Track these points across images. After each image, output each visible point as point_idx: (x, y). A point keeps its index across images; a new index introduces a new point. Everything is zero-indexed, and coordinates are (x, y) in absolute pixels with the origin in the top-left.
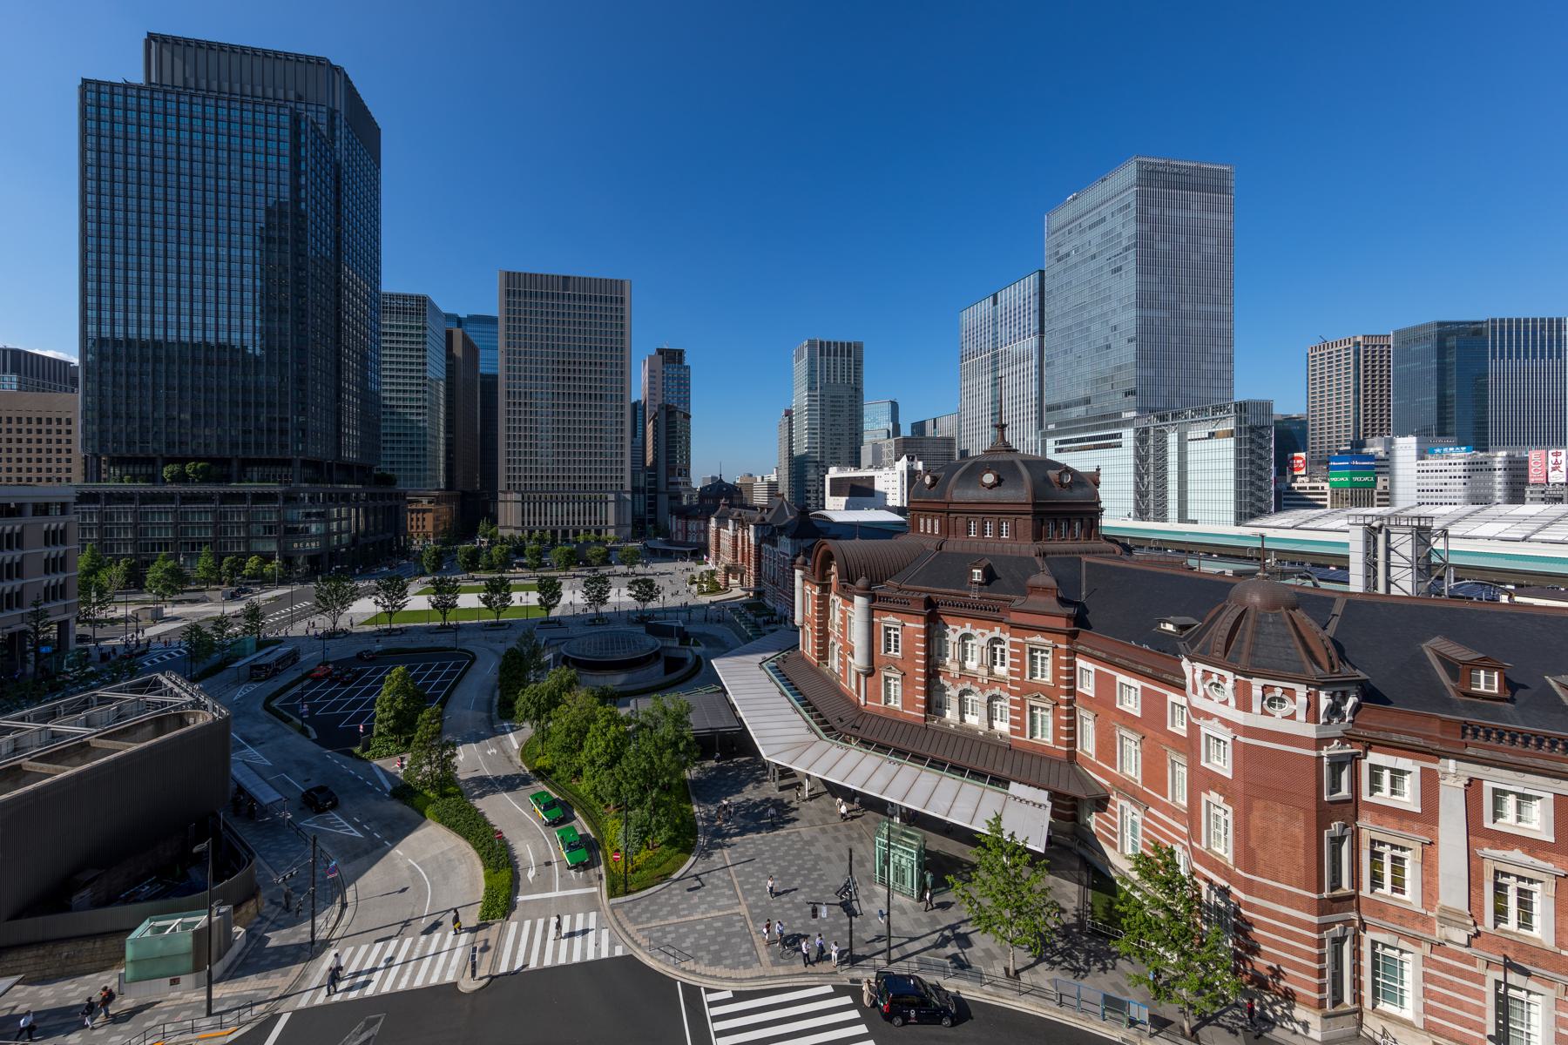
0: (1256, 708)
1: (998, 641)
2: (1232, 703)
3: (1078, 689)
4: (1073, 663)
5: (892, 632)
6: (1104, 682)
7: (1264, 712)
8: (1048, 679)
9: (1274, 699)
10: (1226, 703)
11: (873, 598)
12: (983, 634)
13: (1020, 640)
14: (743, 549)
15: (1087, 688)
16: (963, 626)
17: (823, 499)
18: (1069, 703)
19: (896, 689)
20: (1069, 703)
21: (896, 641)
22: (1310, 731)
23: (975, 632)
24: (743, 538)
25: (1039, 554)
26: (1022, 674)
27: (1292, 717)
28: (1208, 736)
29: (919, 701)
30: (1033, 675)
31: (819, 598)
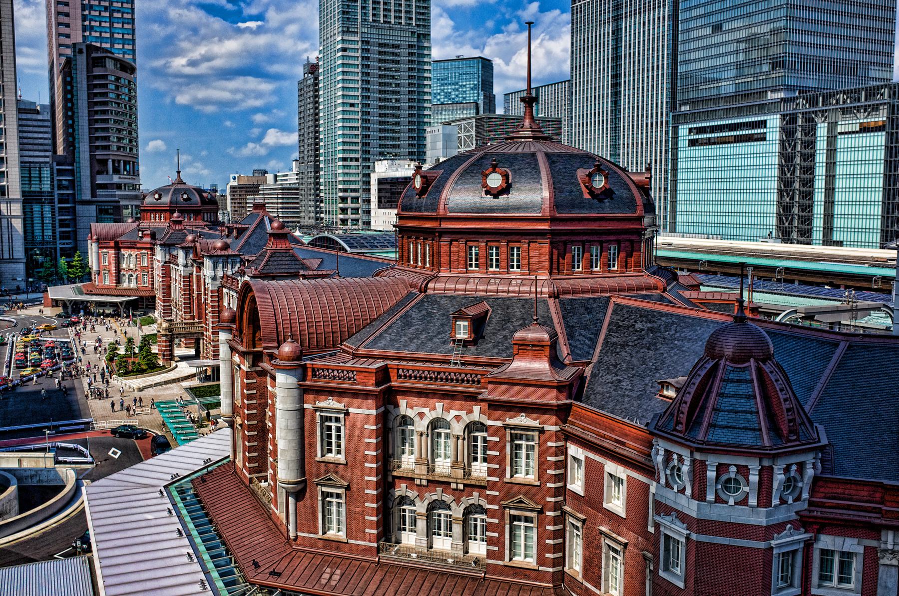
0: (711, 497)
1: (479, 426)
2: (688, 492)
3: (569, 486)
4: (563, 451)
5: (333, 425)
6: (594, 475)
7: (718, 500)
8: (532, 478)
9: (728, 481)
10: (682, 491)
11: (302, 372)
12: (458, 418)
13: (499, 423)
14: (199, 295)
15: (577, 485)
16: (433, 408)
17: (368, 212)
18: (557, 506)
19: (338, 513)
20: (557, 506)
21: (339, 437)
22: (760, 518)
23: (450, 416)
24: (198, 277)
25: (554, 296)
26: (501, 473)
27: (744, 502)
28: (667, 537)
29: (370, 525)
30: (514, 472)
31: (248, 375)
